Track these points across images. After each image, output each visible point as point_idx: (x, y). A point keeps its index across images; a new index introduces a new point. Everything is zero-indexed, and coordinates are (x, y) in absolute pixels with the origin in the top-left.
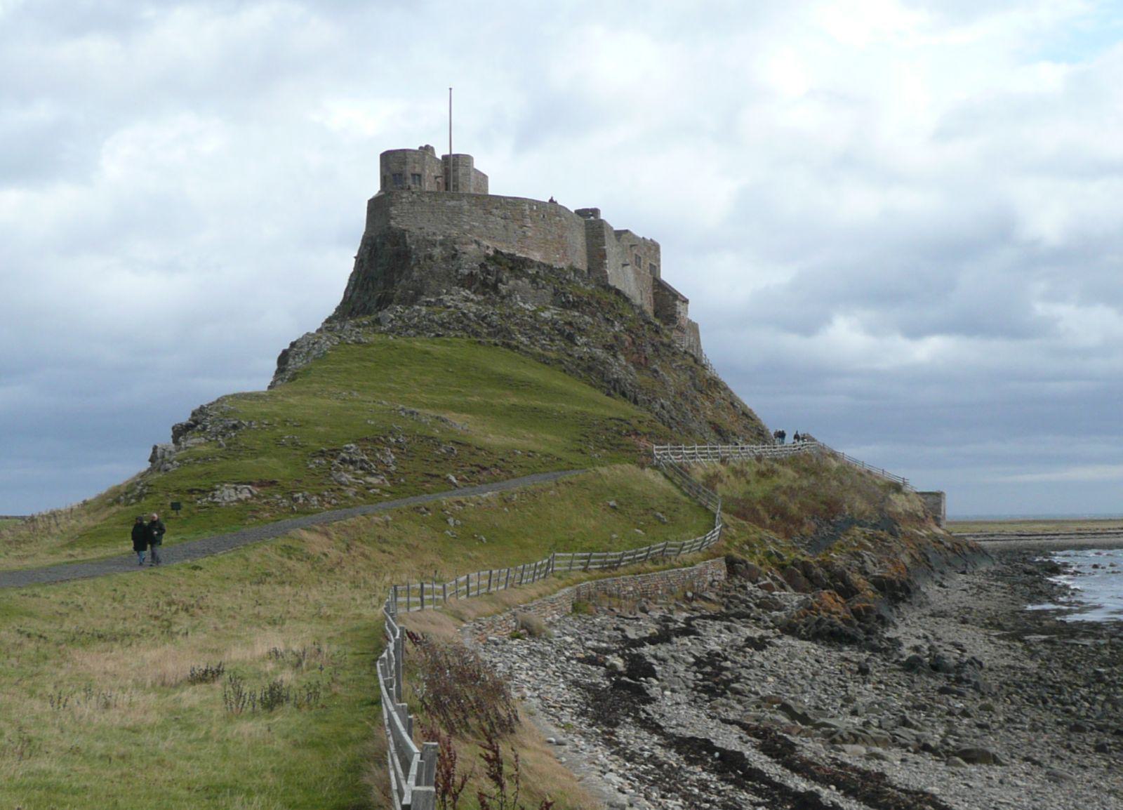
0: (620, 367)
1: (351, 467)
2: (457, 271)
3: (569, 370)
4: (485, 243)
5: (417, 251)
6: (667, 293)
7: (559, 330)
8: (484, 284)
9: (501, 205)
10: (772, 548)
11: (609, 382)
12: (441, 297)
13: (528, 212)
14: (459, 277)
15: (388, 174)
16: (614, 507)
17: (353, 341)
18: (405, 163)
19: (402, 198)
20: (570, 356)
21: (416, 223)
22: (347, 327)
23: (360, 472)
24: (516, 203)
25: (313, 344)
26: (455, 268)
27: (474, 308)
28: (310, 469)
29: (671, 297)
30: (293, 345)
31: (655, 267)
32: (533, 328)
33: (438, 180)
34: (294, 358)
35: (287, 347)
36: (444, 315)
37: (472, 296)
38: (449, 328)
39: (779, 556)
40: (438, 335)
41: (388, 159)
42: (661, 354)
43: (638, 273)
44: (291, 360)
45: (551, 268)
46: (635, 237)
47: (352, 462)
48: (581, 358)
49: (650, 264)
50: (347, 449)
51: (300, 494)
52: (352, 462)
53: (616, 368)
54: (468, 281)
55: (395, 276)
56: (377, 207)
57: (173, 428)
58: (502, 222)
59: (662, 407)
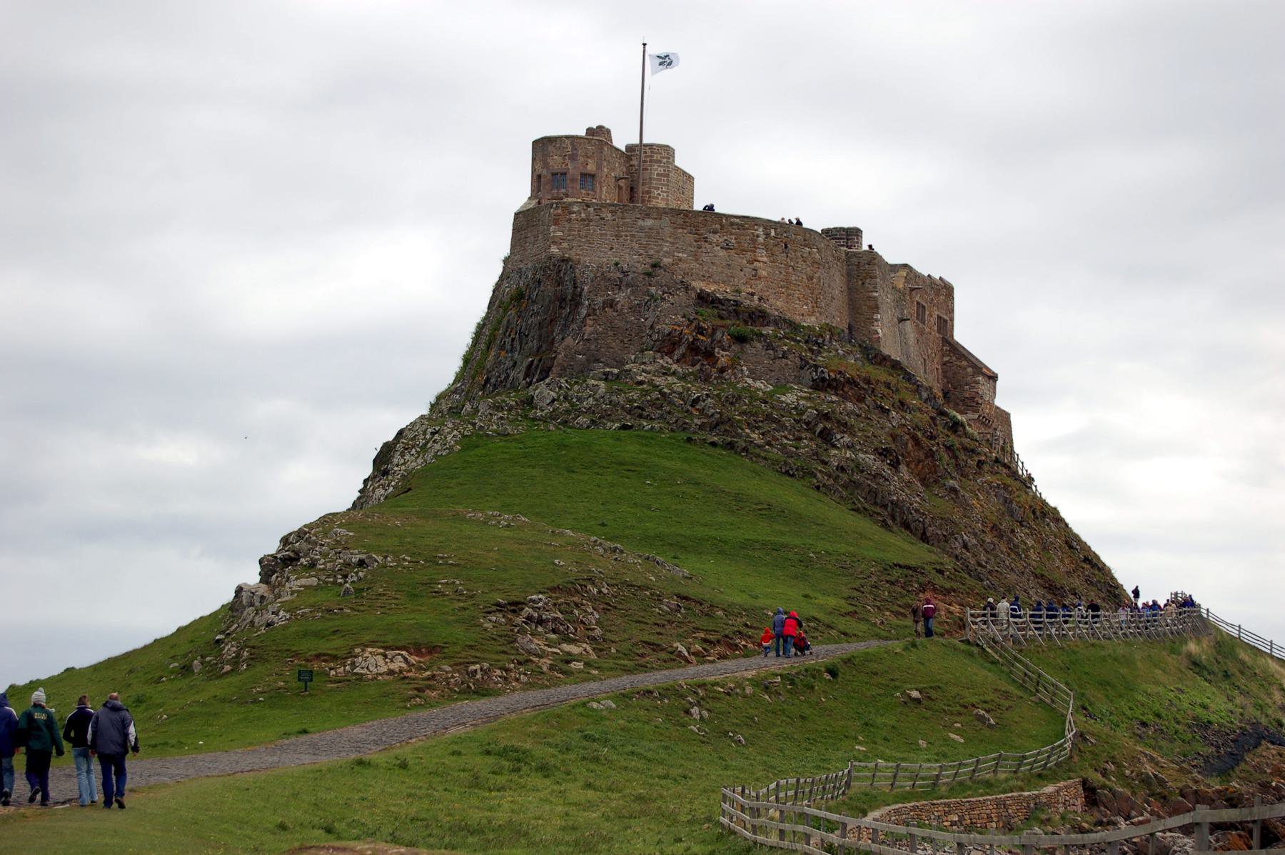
0: (900, 484)
1: (540, 629)
2: (652, 327)
3: (824, 485)
5: (592, 296)
6: (965, 363)
7: (808, 424)
8: (694, 348)
9: (722, 227)
10: (1149, 769)
11: (885, 507)
12: (627, 367)
13: (761, 239)
14: (655, 337)
15: (545, 172)
16: (917, 701)
17: (493, 431)
18: (573, 157)
19: (571, 213)
20: (825, 463)
22: (483, 408)
23: (553, 636)
24: (746, 223)
25: (433, 434)
26: (649, 323)
27: (678, 387)
28: (485, 630)
29: (970, 370)
30: (400, 433)
31: (946, 321)
32: (769, 417)
33: (622, 183)
34: (402, 455)
35: (391, 437)
36: (634, 395)
37: (675, 367)
38: (640, 416)
39: (1161, 782)
40: (624, 427)
41: (543, 147)
42: (963, 464)
43: (921, 332)
44: (397, 456)
45: (794, 326)
46: (918, 276)
47: (541, 622)
48: (842, 469)
49: (939, 317)
50: (533, 601)
51: (478, 666)
52: (541, 622)
53: (895, 483)
54: (668, 345)
55: (557, 329)
56: (524, 223)
57: (261, 562)
58: (722, 253)
59: (965, 546)
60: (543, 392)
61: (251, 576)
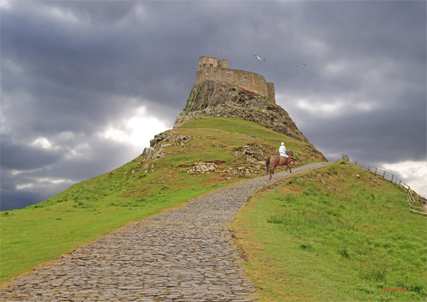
4: (240, 86)
47: (250, 154)
52: (250, 154)
60: (208, 110)
61: (148, 145)
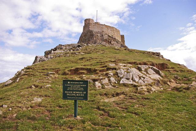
8: (108, 42)
21: (95, 30)
